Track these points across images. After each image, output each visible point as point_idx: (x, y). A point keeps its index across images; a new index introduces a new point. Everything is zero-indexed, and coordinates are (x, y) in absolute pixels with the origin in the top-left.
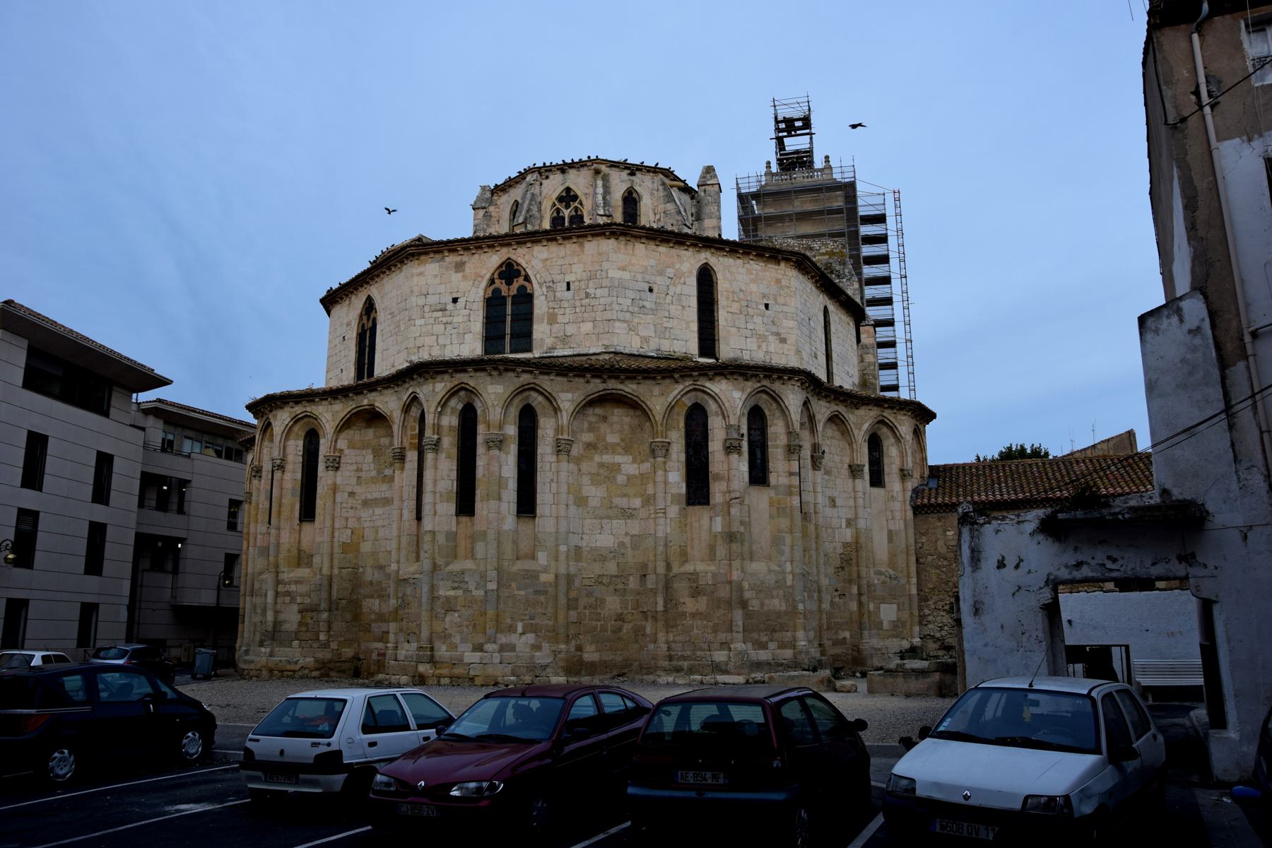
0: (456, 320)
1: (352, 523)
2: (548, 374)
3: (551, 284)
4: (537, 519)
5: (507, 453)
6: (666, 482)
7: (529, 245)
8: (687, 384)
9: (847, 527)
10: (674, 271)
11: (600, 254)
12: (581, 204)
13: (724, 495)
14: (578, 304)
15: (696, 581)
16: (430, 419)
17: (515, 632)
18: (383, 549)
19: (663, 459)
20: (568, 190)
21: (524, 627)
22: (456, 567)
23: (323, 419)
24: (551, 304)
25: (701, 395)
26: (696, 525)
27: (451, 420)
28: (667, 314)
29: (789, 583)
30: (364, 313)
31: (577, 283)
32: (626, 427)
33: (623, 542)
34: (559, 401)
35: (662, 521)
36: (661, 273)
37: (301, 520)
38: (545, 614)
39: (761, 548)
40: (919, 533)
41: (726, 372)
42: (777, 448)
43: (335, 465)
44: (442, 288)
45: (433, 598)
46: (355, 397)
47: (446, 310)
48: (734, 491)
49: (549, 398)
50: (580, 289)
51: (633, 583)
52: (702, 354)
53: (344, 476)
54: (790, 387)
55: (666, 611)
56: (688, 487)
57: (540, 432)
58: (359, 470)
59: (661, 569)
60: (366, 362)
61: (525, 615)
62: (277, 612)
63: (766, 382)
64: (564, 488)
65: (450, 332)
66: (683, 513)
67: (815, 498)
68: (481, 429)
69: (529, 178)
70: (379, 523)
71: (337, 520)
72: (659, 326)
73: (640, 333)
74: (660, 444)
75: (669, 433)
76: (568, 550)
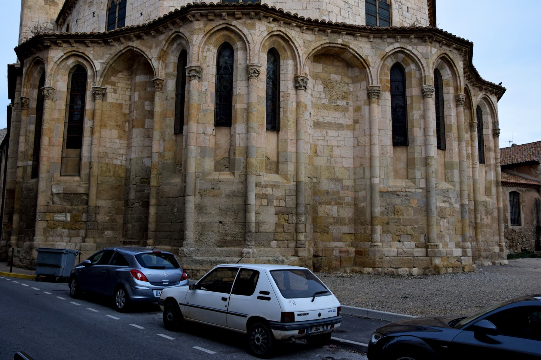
18: (339, 165)
53: (306, 97)
70: (335, 143)
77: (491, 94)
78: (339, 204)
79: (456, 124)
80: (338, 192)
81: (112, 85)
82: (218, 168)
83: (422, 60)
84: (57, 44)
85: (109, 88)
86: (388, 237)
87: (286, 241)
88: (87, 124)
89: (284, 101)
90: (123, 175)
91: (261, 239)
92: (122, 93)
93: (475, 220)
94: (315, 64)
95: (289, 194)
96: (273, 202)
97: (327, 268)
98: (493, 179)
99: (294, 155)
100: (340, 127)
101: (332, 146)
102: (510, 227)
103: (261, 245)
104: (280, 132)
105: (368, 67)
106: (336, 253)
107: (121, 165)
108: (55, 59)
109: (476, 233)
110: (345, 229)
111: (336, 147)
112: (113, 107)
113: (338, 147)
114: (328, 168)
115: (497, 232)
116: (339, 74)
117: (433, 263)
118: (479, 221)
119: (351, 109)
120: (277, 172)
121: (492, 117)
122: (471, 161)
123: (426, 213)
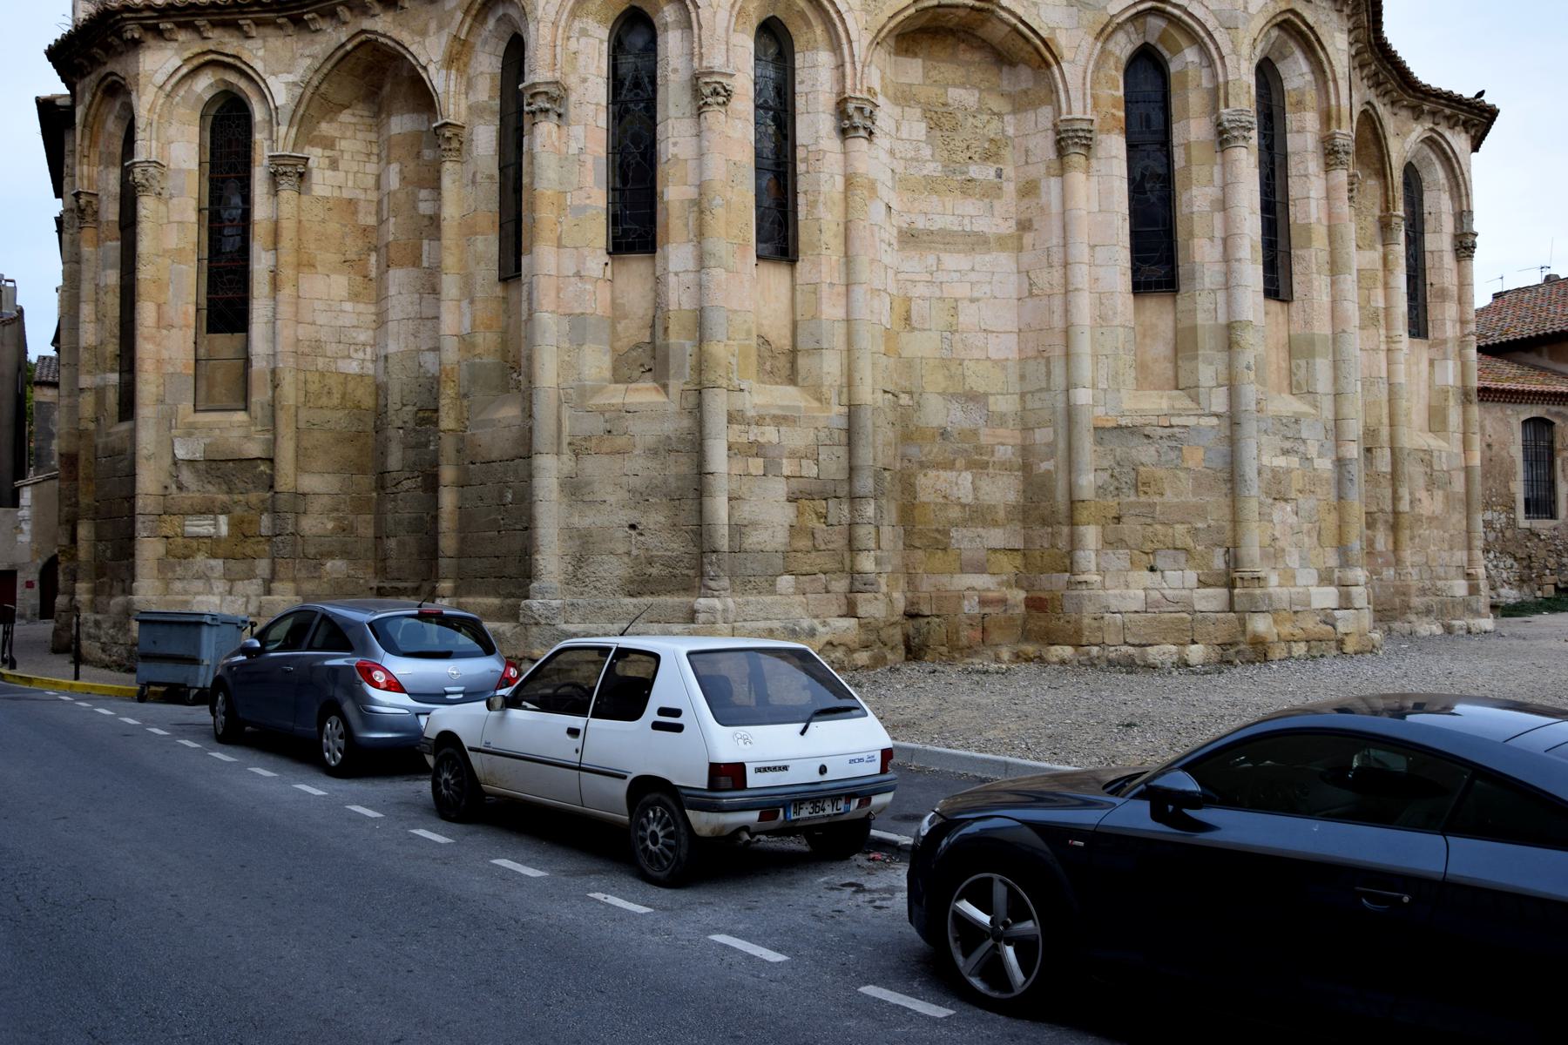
18: (977, 354)
53: (871, 159)
70: (962, 291)
77: (1452, 128)
78: (978, 464)
79: (1325, 222)
80: (975, 432)
81: (325, 148)
82: (622, 372)
83: (1216, 35)
84: (160, 34)
85: (316, 155)
86: (1119, 558)
87: (822, 576)
88: (261, 262)
89: (808, 172)
90: (368, 402)
91: (750, 572)
92: (356, 169)
93: (1394, 505)
94: (900, 59)
95: (828, 442)
96: (780, 465)
97: (944, 649)
98: (1451, 382)
99: (840, 330)
100: (977, 242)
101: (956, 300)
102: (1523, 523)
103: (750, 586)
104: (799, 264)
105: (1058, 63)
106: (970, 607)
107: (361, 376)
108: (160, 78)
109: (1396, 543)
110: (997, 537)
111: (966, 303)
112: (330, 209)
113: (972, 300)
114: (944, 363)
115: (1462, 538)
116: (974, 86)
117: (1250, 627)
118: (1404, 506)
119: (1010, 188)
120: (792, 379)
121: (1452, 197)
122: (1382, 332)
123: (1229, 485)
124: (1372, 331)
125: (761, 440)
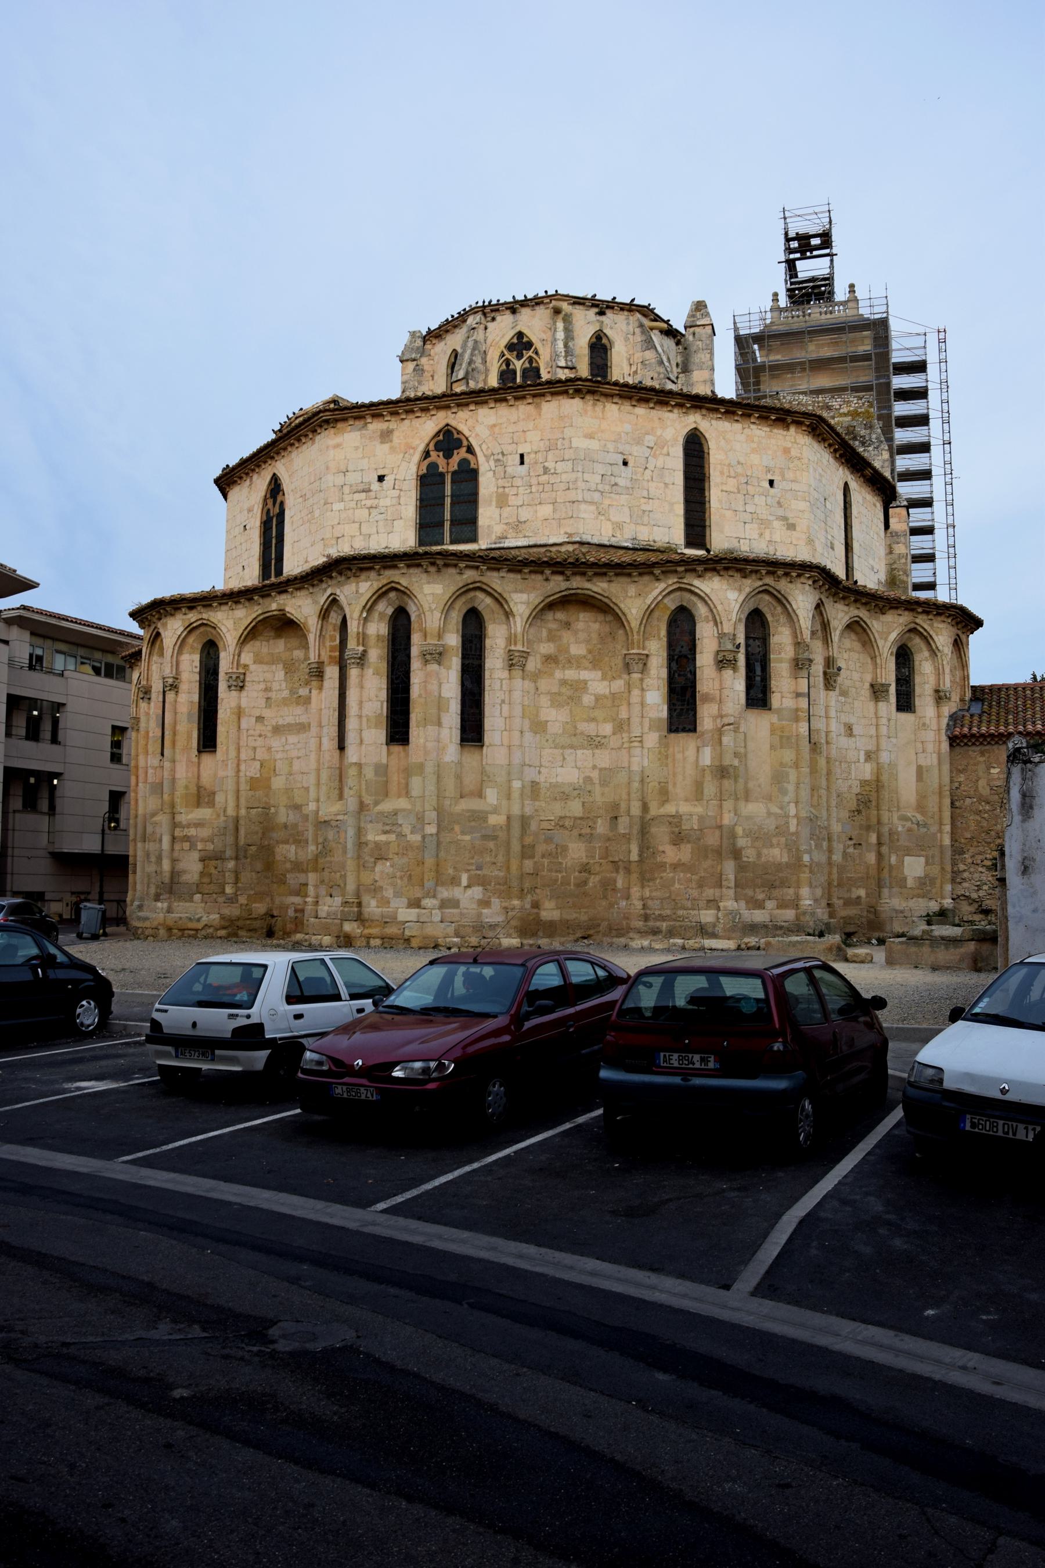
0: (382, 502)
1: (261, 754)
2: (498, 570)
3: (500, 456)
4: (485, 748)
5: (449, 668)
6: (643, 704)
7: (472, 407)
8: (670, 582)
9: (866, 761)
10: (655, 439)
11: (561, 418)
12: (537, 353)
13: (714, 720)
14: (534, 481)
15: (679, 825)
16: (353, 627)
17: (459, 884)
18: (299, 785)
19: (639, 675)
20: (520, 335)
21: (469, 878)
22: (387, 806)
23: (223, 628)
24: (501, 483)
25: (687, 595)
26: (679, 756)
27: (378, 628)
28: (645, 494)
29: (793, 828)
30: (268, 496)
31: (533, 456)
32: (594, 636)
33: (589, 777)
34: (511, 604)
35: (637, 751)
36: (639, 441)
37: (199, 752)
38: (495, 863)
39: (759, 786)
40: (955, 770)
41: (719, 567)
42: (781, 662)
43: (239, 684)
44: (364, 464)
45: (360, 844)
46: (261, 601)
47: (370, 491)
48: (726, 716)
49: (500, 600)
50: (536, 463)
51: (601, 827)
52: (689, 544)
53: (251, 698)
54: (799, 586)
55: (641, 861)
56: (671, 710)
57: (488, 642)
58: (267, 690)
59: (636, 810)
60: (273, 556)
61: (472, 864)
62: (174, 861)
63: (769, 580)
64: (518, 711)
65: (376, 518)
66: (663, 743)
67: (828, 725)
68: (416, 638)
69: (471, 320)
70: (294, 753)
71: (243, 750)
72: (636, 509)
73: (611, 517)
74: (636, 657)
75: (647, 643)
76: (523, 787)
80: (296, 825)
87: (214, 895)
96: (196, 845)
111: (295, 760)
124: (618, 736)
125: (189, 834)
